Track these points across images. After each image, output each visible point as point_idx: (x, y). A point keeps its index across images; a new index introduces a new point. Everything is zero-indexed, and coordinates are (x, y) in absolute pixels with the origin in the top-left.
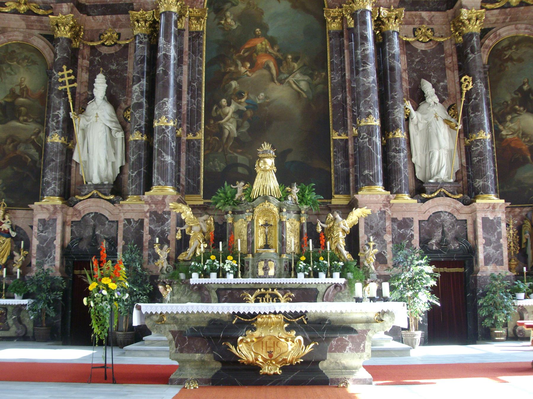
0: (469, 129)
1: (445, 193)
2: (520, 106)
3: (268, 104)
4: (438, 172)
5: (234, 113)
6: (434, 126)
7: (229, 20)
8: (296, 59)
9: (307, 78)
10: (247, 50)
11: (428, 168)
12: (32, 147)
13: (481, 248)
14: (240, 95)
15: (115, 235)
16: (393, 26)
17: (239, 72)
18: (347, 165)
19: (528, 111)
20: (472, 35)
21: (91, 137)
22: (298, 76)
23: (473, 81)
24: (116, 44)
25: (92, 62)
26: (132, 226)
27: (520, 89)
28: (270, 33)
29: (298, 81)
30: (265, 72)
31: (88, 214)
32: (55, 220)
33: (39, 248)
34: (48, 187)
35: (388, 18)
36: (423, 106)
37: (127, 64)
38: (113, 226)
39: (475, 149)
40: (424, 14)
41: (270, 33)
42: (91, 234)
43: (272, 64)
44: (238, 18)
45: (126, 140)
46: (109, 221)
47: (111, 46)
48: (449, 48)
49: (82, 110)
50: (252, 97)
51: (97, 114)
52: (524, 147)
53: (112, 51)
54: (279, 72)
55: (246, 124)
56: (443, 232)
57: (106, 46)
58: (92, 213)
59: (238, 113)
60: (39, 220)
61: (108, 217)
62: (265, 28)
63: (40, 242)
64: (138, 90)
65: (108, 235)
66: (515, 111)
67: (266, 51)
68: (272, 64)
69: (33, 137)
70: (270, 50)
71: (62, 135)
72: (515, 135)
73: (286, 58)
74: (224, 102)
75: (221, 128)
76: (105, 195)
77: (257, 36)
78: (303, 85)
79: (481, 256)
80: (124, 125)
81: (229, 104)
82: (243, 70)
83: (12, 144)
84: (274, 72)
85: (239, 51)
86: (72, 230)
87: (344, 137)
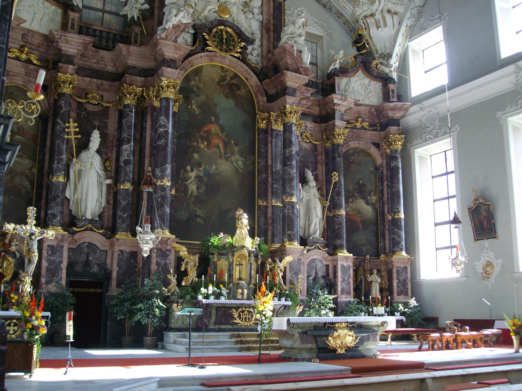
1: (318, 247)
2: (357, 194)
3: (218, 174)
4: (315, 233)
5: (196, 177)
6: (313, 202)
7: (194, 107)
8: (236, 144)
9: (243, 159)
10: (205, 132)
11: (307, 229)
12: (26, 180)
13: (339, 284)
14: (199, 165)
15: (104, 262)
17: (199, 147)
18: (266, 224)
19: (361, 197)
21: (86, 180)
22: (237, 157)
23: (339, 176)
24: (99, 104)
25: (78, 115)
26: (125, 256)
27: (358, 183)
28: (221, 122)
29: (237, 160)
30: (216, 150)
31: (83, 243)
32: (62, 247)
33: (47, 269)
34: (55, 219)
37: (107, 122)
38: (102, 255)
39: (336, 220)
41: (221, 122)
42: (85, 259)
43: (221, 145)
44: (201, 106)
46: (100, 250)
47: (95, 105)
50: (207, 167)
51: (92, 162)
52: (358, 220)
53: (96, 109)
54: (225, 152)
55: (203, 187)
56: (316, 272)
57: (91, 104)
58: (86, 243)
59: (198, 177)
60: (49, 246)
61: (100, 247)
62: (217, 117)
63: (49, 265)
65: (98, 261)
66: (354, 196)
67: (218, 134)
68: (221, 145)
69: (27, 171)
70: (220, 135)
72: (354, 212)
73: (230, 142)
74: (189, 168)
75: (186, 188)
76: (99, 230)
77: (212, 123)
78: (240, 163)
81: (192, 171)
82: (202, 146)
83: (10, 175)
84: (222, 151)
85: (199, 132)
86: (69, 255)
87: (265, 204)
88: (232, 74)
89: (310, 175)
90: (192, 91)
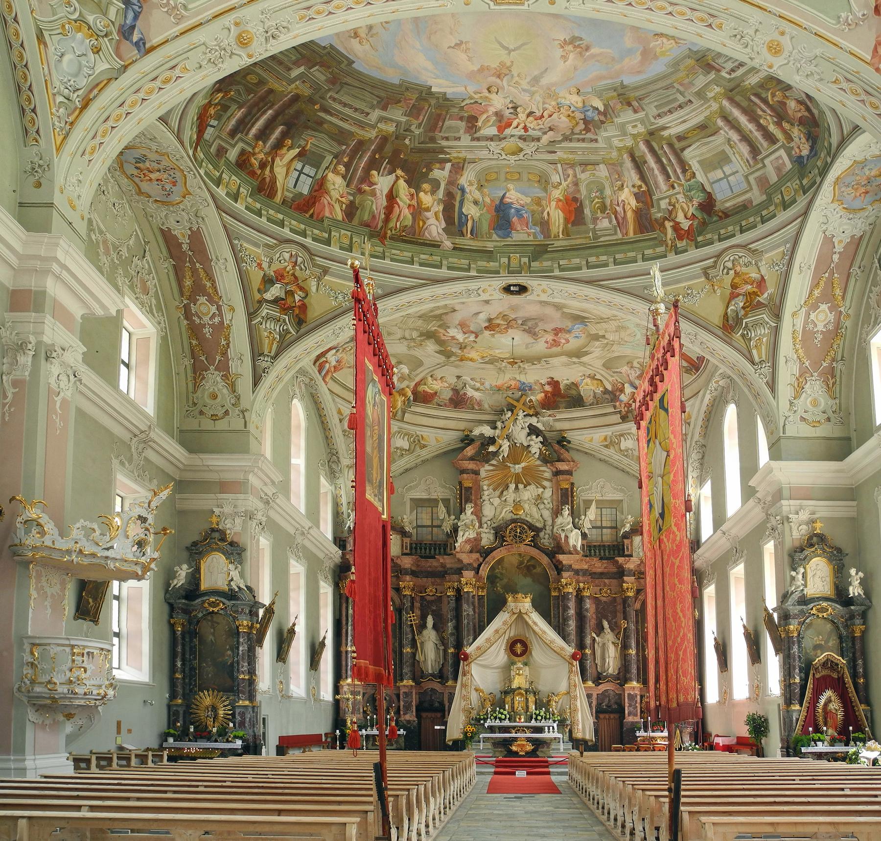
0: (625, 647)
16: (586, 593)
20: (629, 597)
35: (584, 588)
36: (602, 634)
40: (606, 581)
45: (445, 651)
48: (619, 600)
49: (420, 633)
53: (433, 598)
64: (450, 625)
71: (411, 648)
79: (626, 712)
80: (443, 640)
88: (528, 558)
89: (606, 624)
90: (496, 577)
